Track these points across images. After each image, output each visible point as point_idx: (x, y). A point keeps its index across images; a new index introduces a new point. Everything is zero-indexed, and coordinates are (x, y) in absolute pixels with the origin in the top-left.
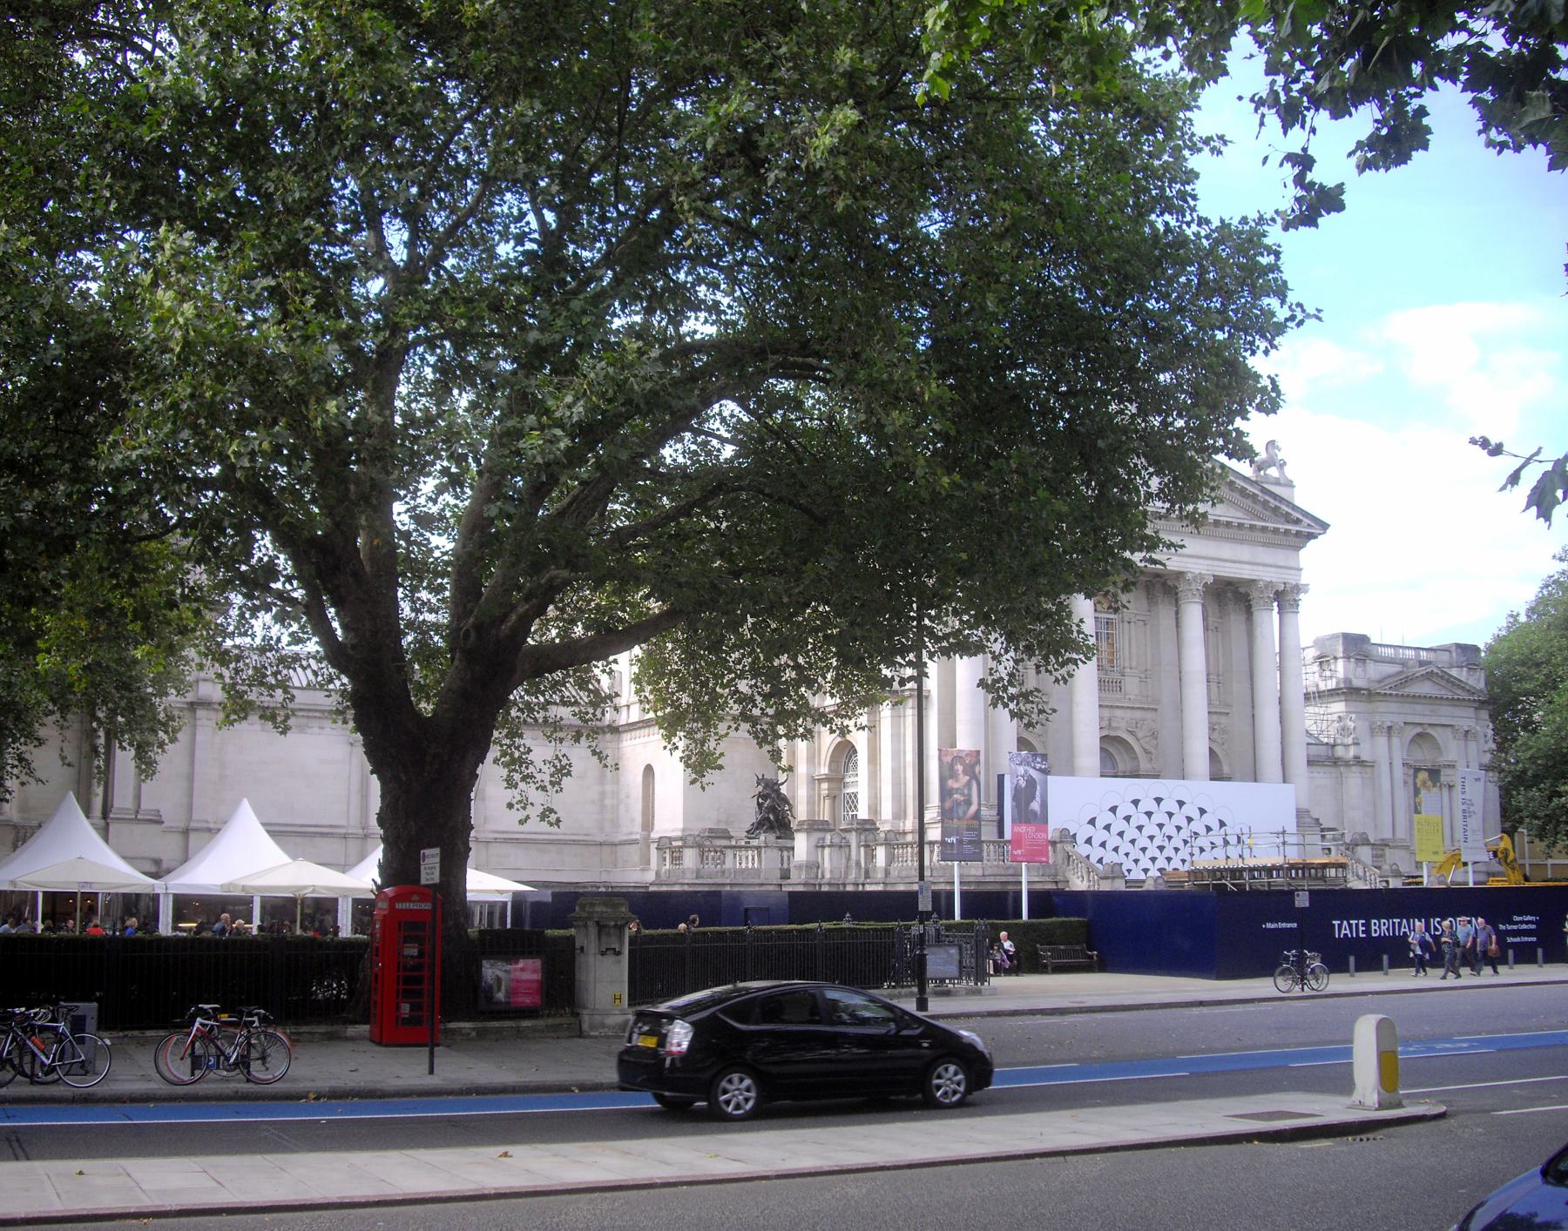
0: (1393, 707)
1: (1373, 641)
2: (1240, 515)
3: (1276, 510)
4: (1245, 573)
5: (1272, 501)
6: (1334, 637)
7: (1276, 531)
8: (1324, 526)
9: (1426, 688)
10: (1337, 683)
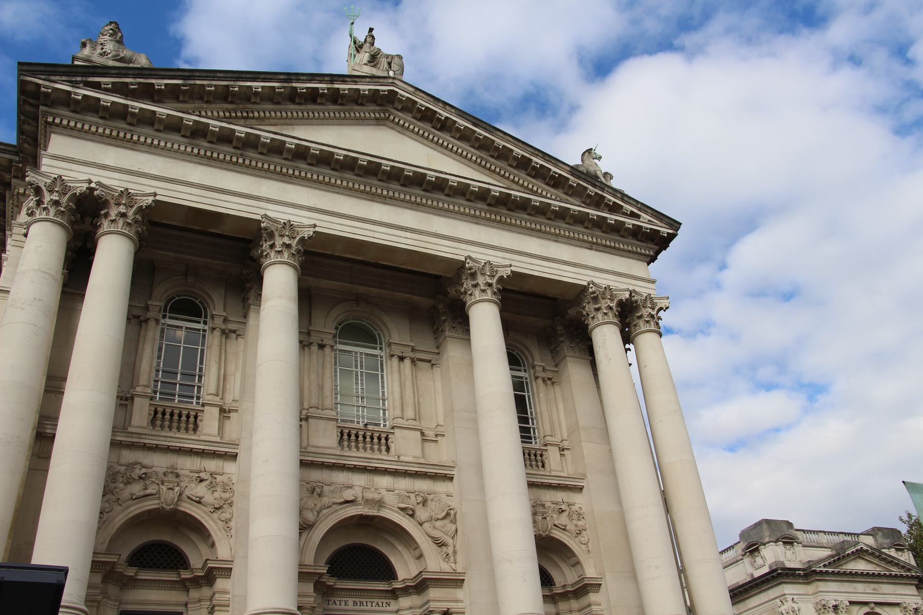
0: (833, 586)
1: (796, 527)
5: (590, 187)
6: (759, 524)
8: (675, 225)
9: (860, 566)
10: (770, 567)
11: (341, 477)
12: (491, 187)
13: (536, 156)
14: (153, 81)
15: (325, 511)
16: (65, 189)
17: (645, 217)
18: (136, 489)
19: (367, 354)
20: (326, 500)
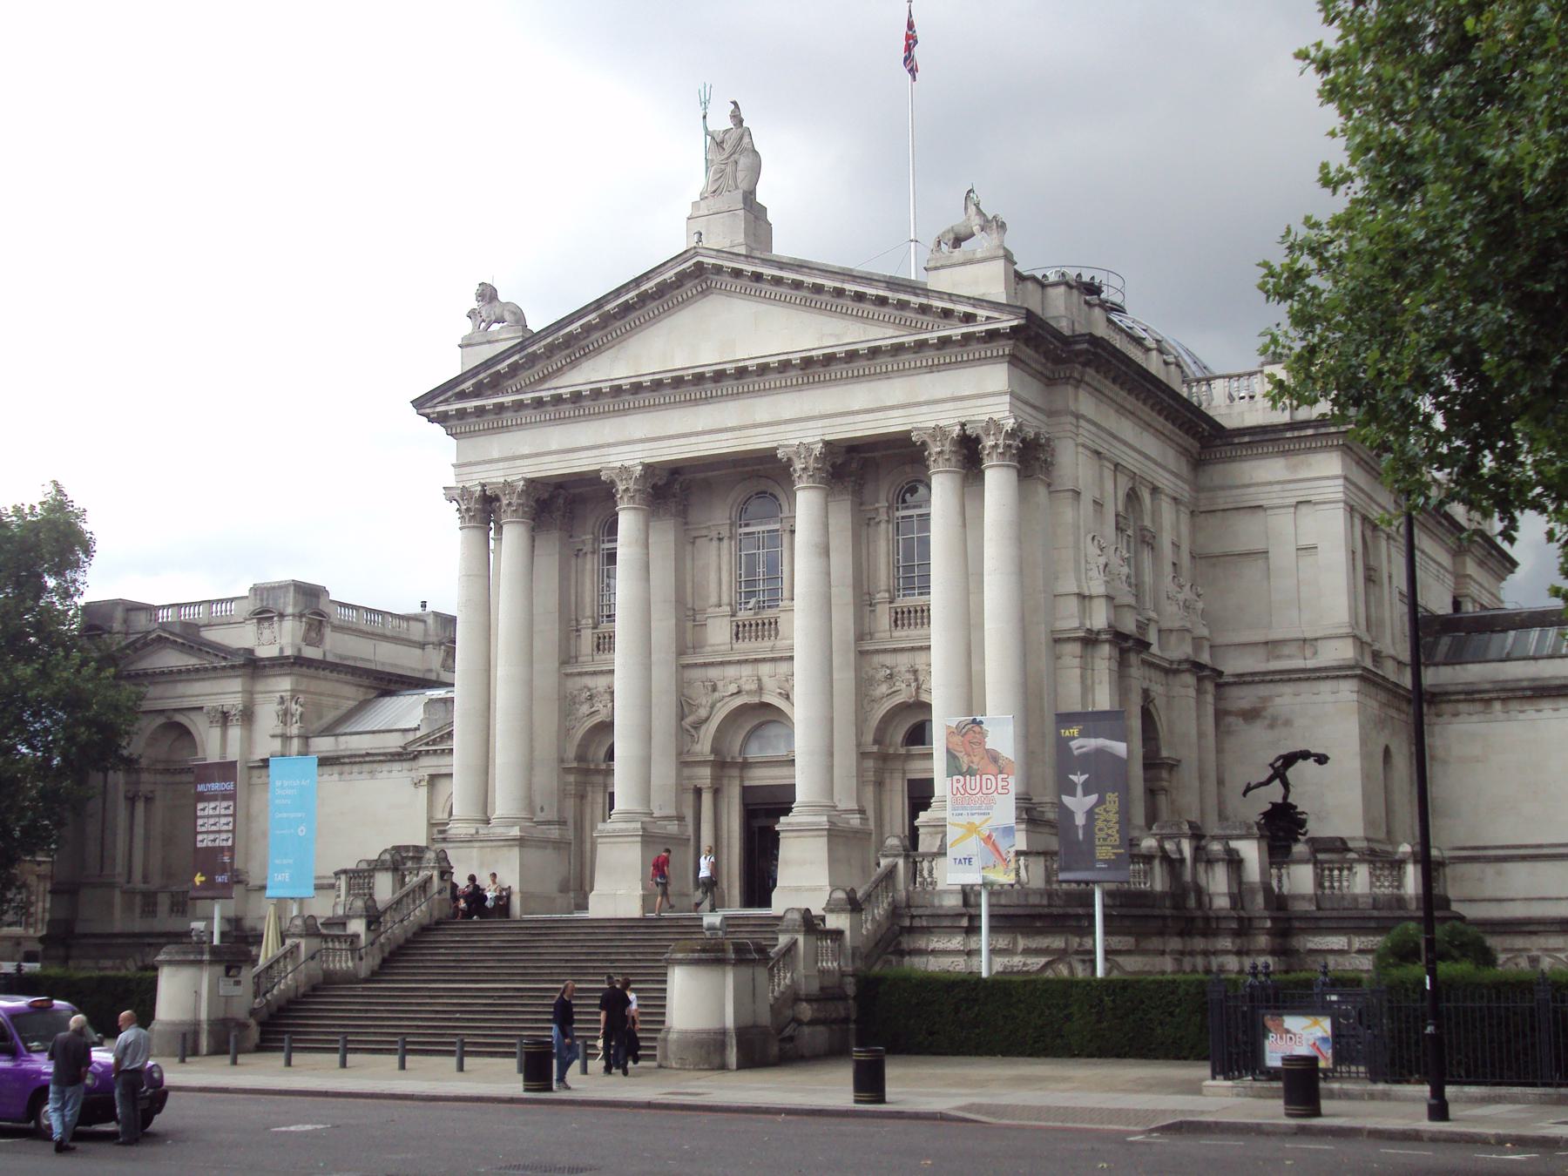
2: (890, 332)
3: (947, 314)
4: (891, 424)
7: (945, 342)
11: (731, 671)
12: (790, 356)
13: (848, 282)
14: (499, 367)
15: (719, 705)
16: (471, 494)
17: (982, 313)
18: (585, 709)
19: (769, 531)
20: (717, 695)
